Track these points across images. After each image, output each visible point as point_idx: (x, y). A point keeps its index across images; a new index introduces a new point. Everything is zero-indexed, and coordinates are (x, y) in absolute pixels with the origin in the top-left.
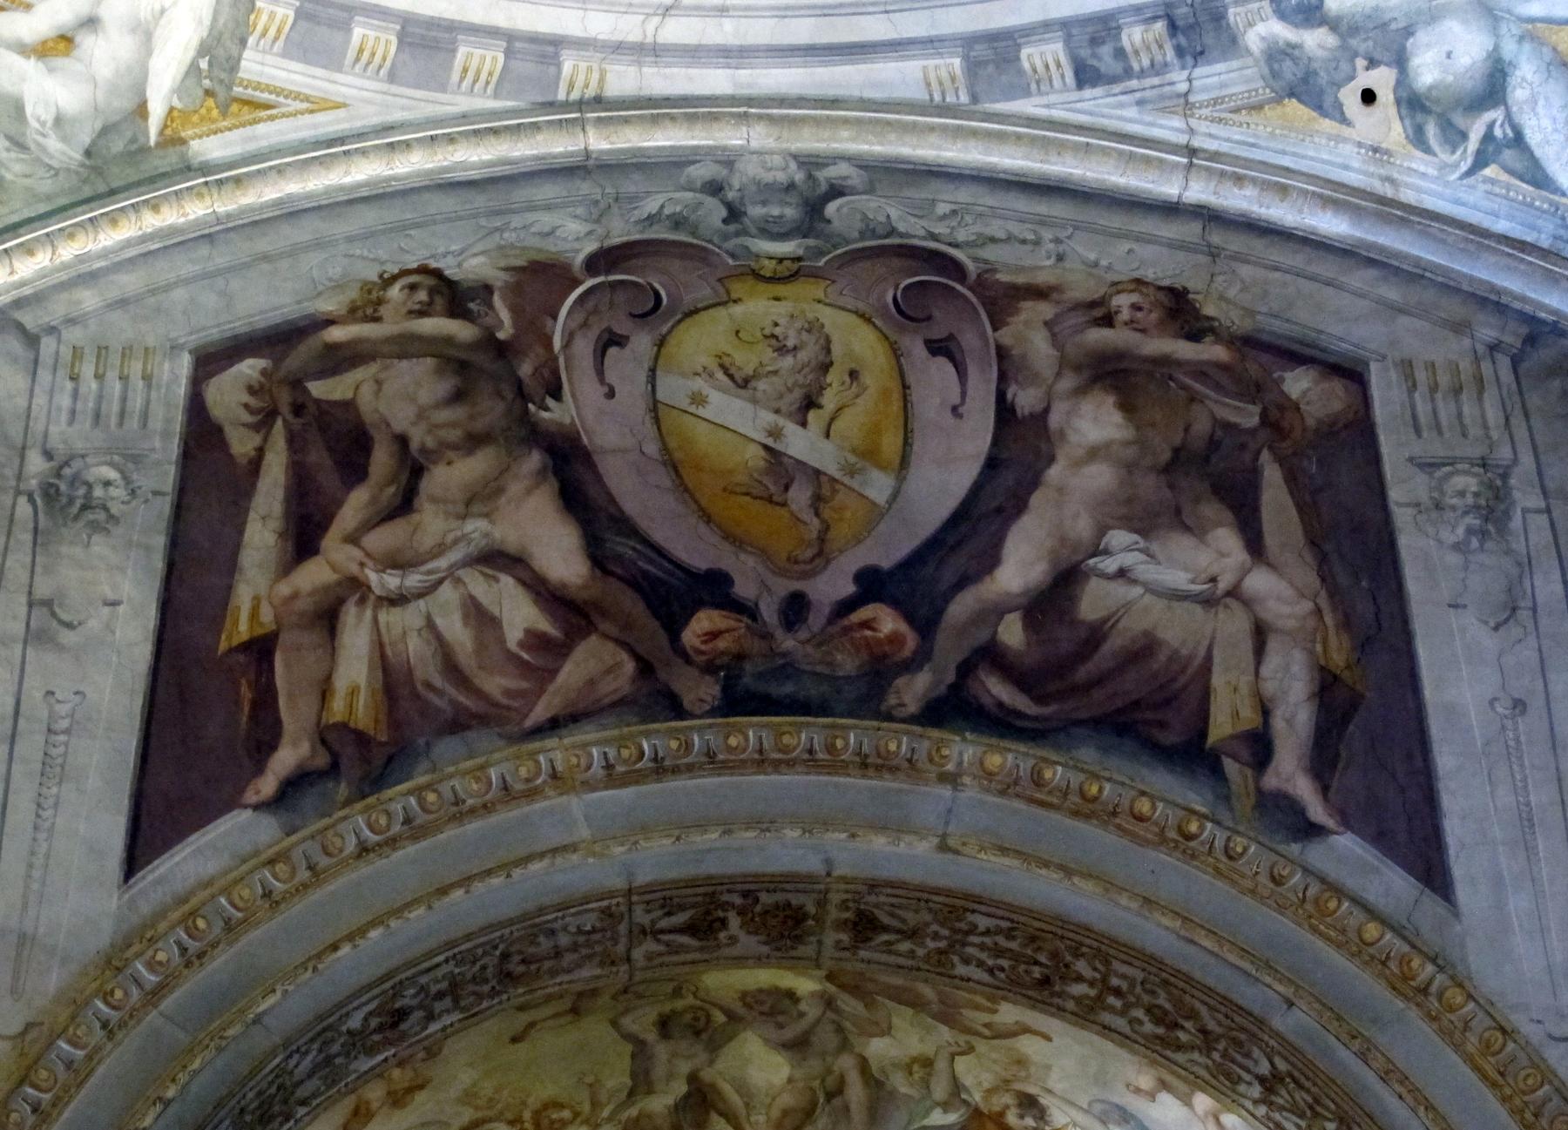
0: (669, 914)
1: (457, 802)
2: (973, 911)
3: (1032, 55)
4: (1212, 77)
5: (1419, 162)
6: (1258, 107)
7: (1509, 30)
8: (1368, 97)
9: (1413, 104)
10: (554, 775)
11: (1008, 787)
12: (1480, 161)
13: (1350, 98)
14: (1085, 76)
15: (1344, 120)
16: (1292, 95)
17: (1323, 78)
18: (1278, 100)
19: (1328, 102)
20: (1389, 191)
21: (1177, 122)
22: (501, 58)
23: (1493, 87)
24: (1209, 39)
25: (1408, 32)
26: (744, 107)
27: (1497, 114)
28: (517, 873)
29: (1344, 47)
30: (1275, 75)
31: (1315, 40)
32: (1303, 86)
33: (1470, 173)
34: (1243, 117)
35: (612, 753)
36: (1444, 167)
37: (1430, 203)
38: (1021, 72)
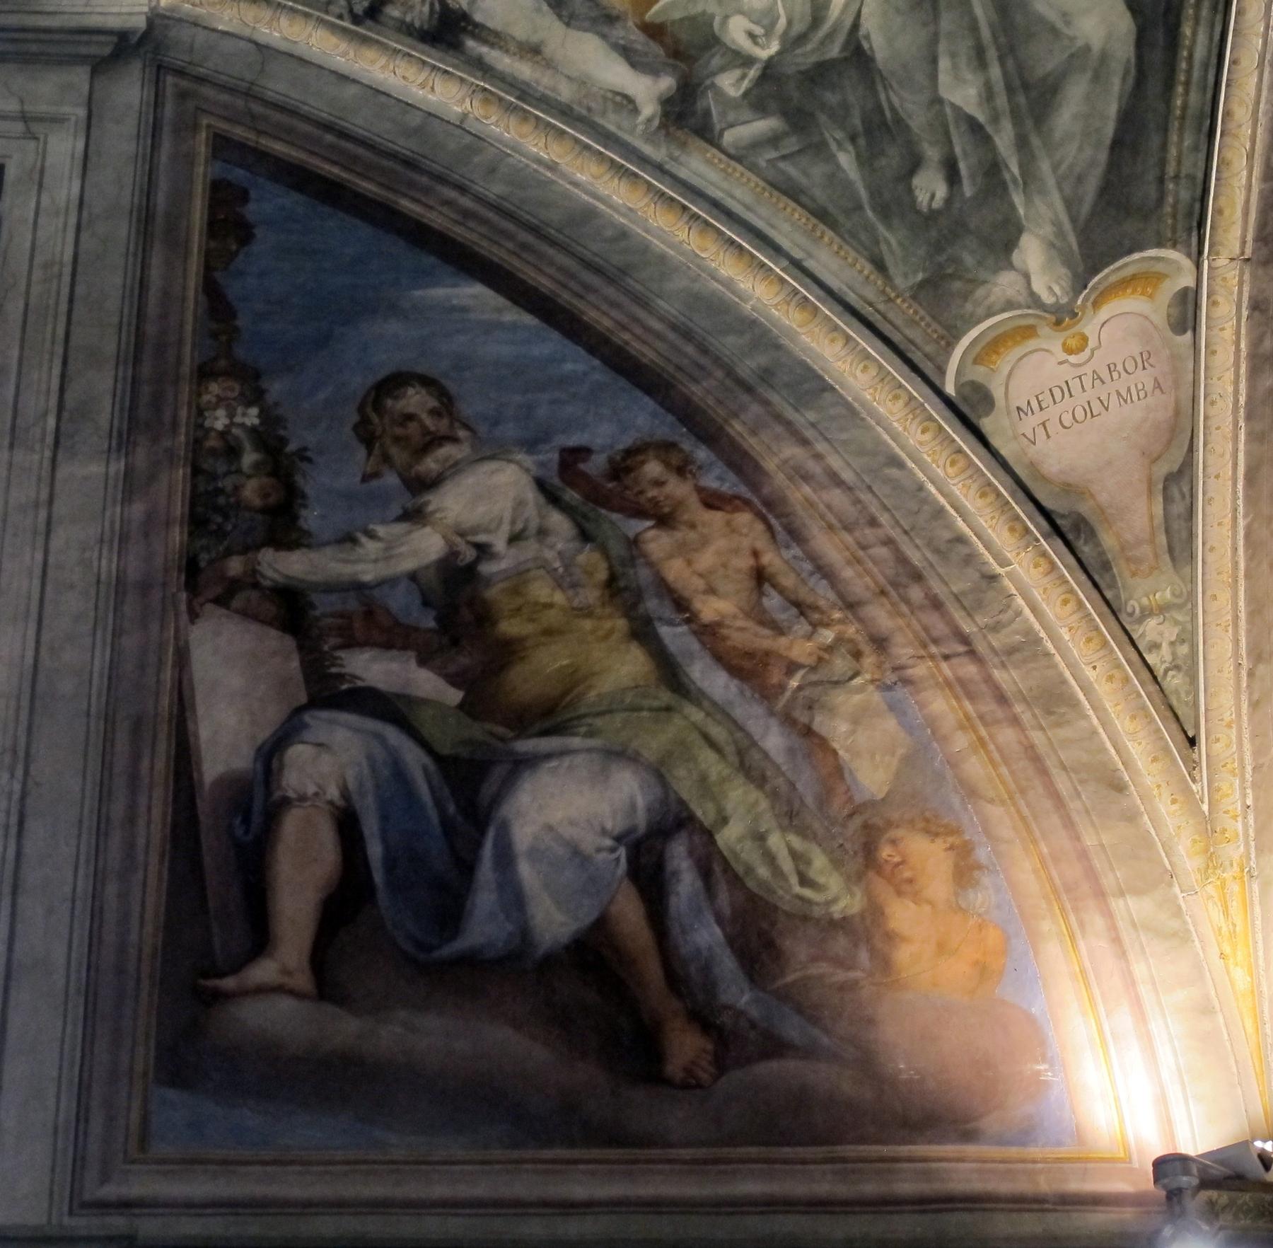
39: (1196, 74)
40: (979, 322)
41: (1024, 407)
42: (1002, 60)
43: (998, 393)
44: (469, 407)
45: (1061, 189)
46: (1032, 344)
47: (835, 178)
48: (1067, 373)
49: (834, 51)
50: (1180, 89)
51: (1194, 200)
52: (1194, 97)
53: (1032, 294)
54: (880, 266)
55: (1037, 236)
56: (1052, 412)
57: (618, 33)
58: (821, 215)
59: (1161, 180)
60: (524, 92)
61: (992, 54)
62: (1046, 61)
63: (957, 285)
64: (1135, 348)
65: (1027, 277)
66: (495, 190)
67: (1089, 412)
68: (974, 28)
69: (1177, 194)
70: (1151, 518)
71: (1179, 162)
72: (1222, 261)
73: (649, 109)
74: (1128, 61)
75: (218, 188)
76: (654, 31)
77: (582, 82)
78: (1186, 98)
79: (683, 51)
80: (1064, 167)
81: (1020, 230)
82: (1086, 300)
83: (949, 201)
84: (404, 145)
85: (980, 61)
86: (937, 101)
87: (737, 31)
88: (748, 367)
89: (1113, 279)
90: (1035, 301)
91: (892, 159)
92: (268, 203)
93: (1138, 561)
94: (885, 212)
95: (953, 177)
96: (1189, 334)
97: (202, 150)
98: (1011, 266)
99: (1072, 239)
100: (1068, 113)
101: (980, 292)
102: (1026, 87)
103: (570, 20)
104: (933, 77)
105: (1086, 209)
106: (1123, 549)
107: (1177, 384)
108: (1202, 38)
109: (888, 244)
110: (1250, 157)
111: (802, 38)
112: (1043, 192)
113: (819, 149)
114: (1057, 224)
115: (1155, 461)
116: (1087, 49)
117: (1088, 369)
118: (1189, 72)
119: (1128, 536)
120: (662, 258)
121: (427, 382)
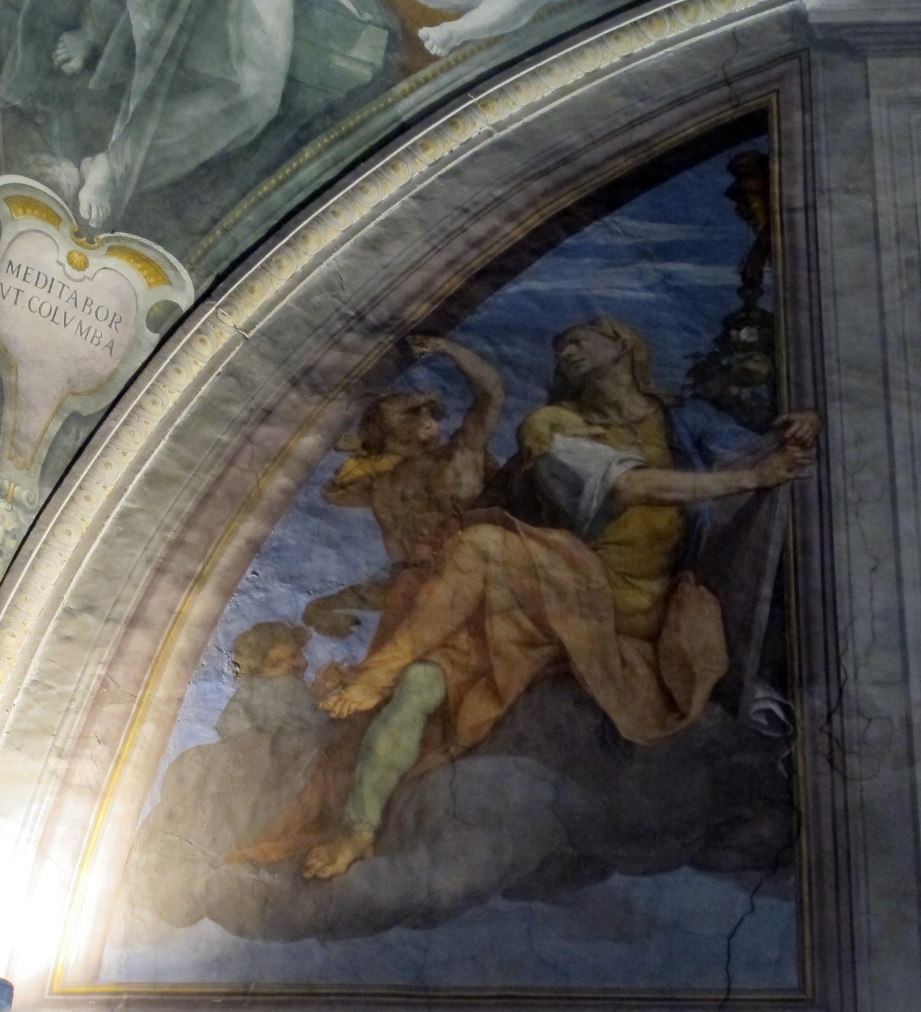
39: (291, 185)
40: (27, 175)
41: (15, 266)
42: (181, 28)
45: (148, 154)
46: (50, 229)
50: (273, 182)
51: (226, 258)
53: (76, 196)
55: (111, 166)
56: (30, 290)
59: (215, 221)
61: (178, 18)
62: (206, 64)
63: (35, 136)
64: (113, 305)
65: (82, 182)
67: (53, 313)
69: (217, 241)
70: (45, 431)
71: (236, 224)
72: (229, 321)
74: (256, 126)
80: (163, 142)
81: (103, 149)
82: (107, 240)
83: (75, 76)
89: (135, 247)
90: (74, 203)
93: (19, 451)
94: (30, 32)
95: (91, 62)
96: (155, 338)
98: (78, 165)
99: (129, 193)
100: (195, 111)
101: (45, 158)
102: (181, 64)
105: (153, 184)
106: (14, 432)
107: (123, 360)
108: (313, 169)
109: (16, 53)
110: (298, 278)
112: (137, 142)
114: (128, 170)
115: (74, 394)
116: (236, 89)
117: (73, 286)
118: (288, 178)
119: (22, 428)
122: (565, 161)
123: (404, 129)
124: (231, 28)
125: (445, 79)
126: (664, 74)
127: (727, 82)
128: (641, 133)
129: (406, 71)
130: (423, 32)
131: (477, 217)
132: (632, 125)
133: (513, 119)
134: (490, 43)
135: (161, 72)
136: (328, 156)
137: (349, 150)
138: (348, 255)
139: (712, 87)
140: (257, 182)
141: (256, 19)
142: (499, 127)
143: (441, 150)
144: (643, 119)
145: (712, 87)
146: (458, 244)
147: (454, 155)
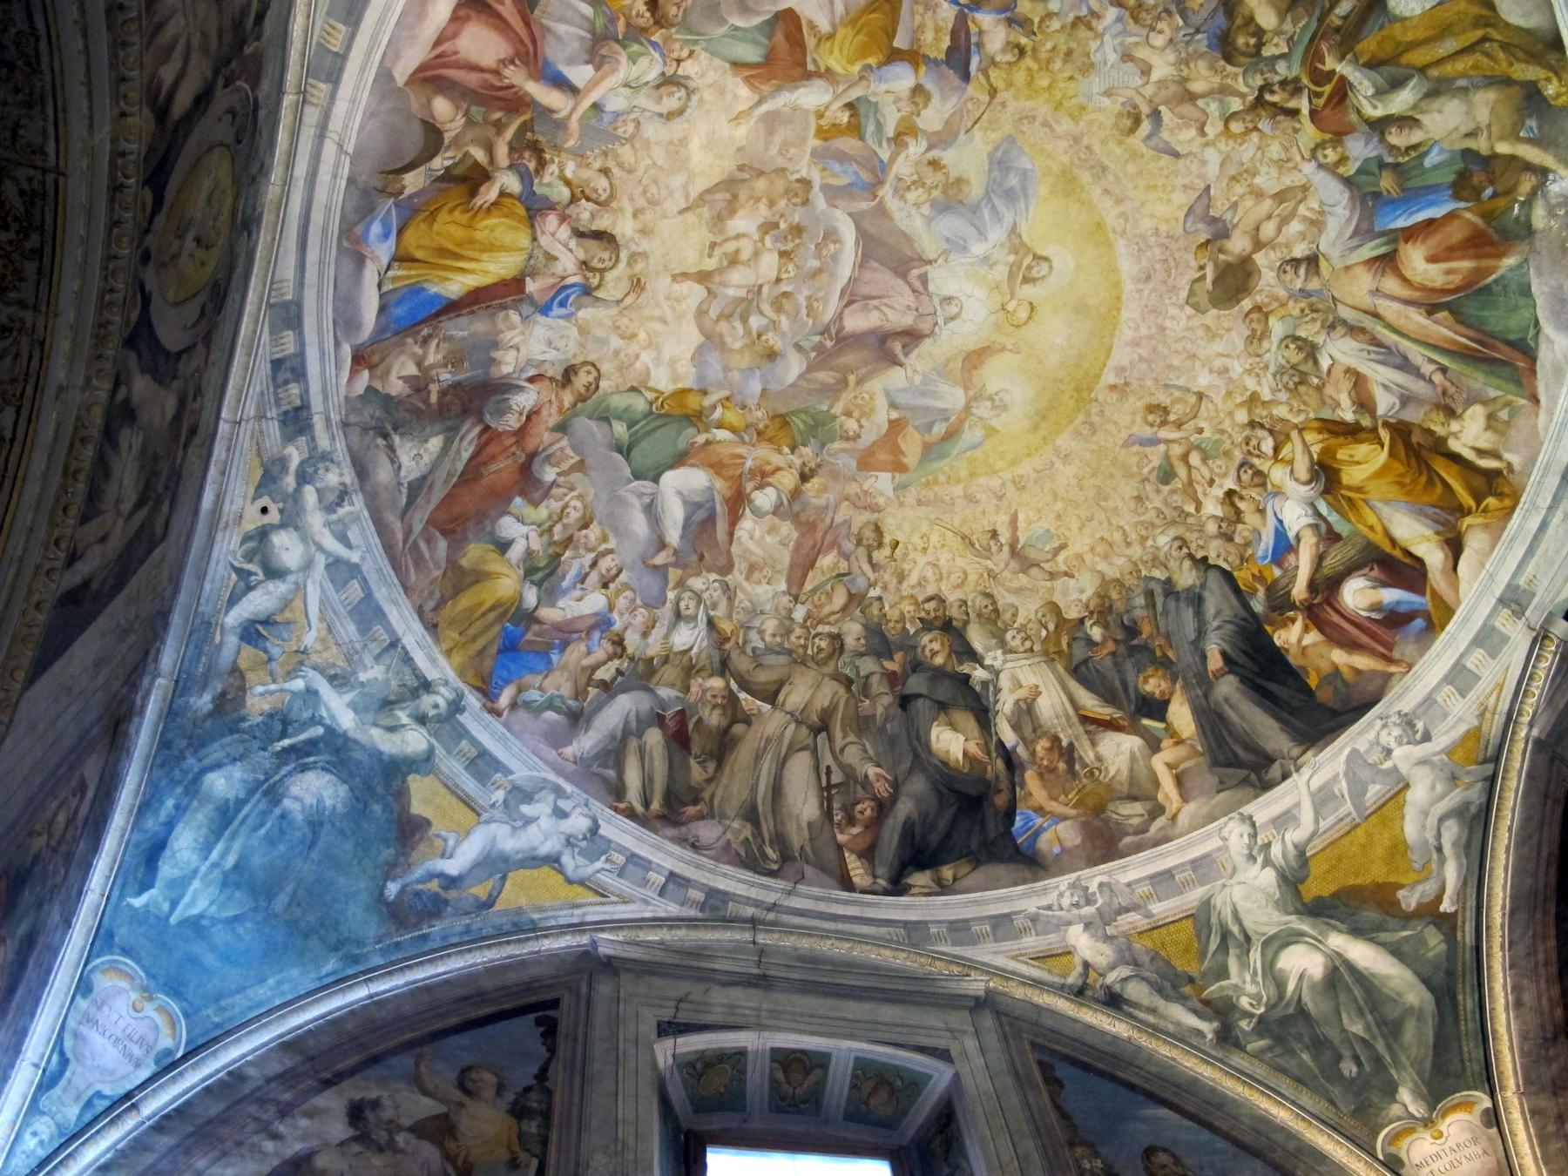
0: (22, 193)
1: (124, 45)
2: (18, 412)
3: (289, 336)
4: (273, 429)
5: (236, 540)
6: (259, 455)
7: (299, 577)
8: (264, 510)
9: (263, 534)
10: (123, 115)
11: (80, 423)
12: (239, 571)
13: (265, 501)
14: (277, 364)
15: (254, 499)
16: (266, 472)
17: (273, 487)
18: (263, 465)
19: (262, 490)
20: (221, 526)
21: (252, 413)
22: (335, 50)
23: (274, 573)
24: (291, 428)
25: (296, 528)
26: (287, 183)
27: (261, 576)
28: (84, 90)
29: (287, 496)
30: (274, 462)
31: (290, 481)
32: (269, 478)
33: (232, 566)
34: (255, 448)
35: (132, 157)
36: (234, 552)
37: (216, 548)
38: (282, 331)
43: (1405, 1158)
44: (1188, 1162)
46: (1415, 1136)
47: (1302, 1064)
48: (1434, 1149)
49: (1291, 1010)
52: (1471, 1026)
54: (1332, 1102)
57: (1190, 1003)
58: (1299, 1081)
59: (1462, 1061)
60: (1155, 1028)
61: (1366, 1011)
62: (1393, 1013)
66: (1153, 1069)
68: (1355, 1000)
73: (1210, 1036)
75: (1040, 1063)
76: (1206, 1003)
77: (1178, 1024)
78: (1469, 1026)
79: (1222, 1011)
83: (1359, 1073)
84: (1107, 1048)
85: (1361, 1012)
86: (1344, 1031)
87: (1244, 1002)
88: (1291, 1146)
90: (1412, 1116)
91: (1328, 1055)
92: (1063, 1071)
94: (1328, 1079)
95: (1359, 1064)
97: (1028, 1047)
98: (1396, 1101)
99: (1424, 1089)
100: (1410, 1032)
102: (1386, 1024)
103: (1167, 998)
104: (1340, 1019)
108: (1469, 1001)
110: (1511, 1048)
111: (1275, 1006)
112: (1405, 1068)
113: (1292, 1052)
114: (1413, 1081)
116: (1412, 1007)
120: (1234, 1100)
121: (1165, 1150)
122: (1536, 894)
123: (1478, 949)
124: (1385, 990)
125: (1468, 914)
126: (1526, 821)
127: (1546, 796)
128: (1544, 854)
129: (1454, 928)
130: (1442, 909)
131: (1535, 953)
132: (1539, 853)
133: (1504, 899)
134: (1465, 884)
135: (1383, 1036)
136: (1468, 990)
137: (1471, 979)
138: (1517, 1017)
139: (1545, 805)
140: (1458, 1030)
141: (1388, 977)
142: (1503, 908)
143: (1497, 941)
144: (1539, 843)
145: (1545, 805)
146: (1542, 971)
147: (1503, 936)
